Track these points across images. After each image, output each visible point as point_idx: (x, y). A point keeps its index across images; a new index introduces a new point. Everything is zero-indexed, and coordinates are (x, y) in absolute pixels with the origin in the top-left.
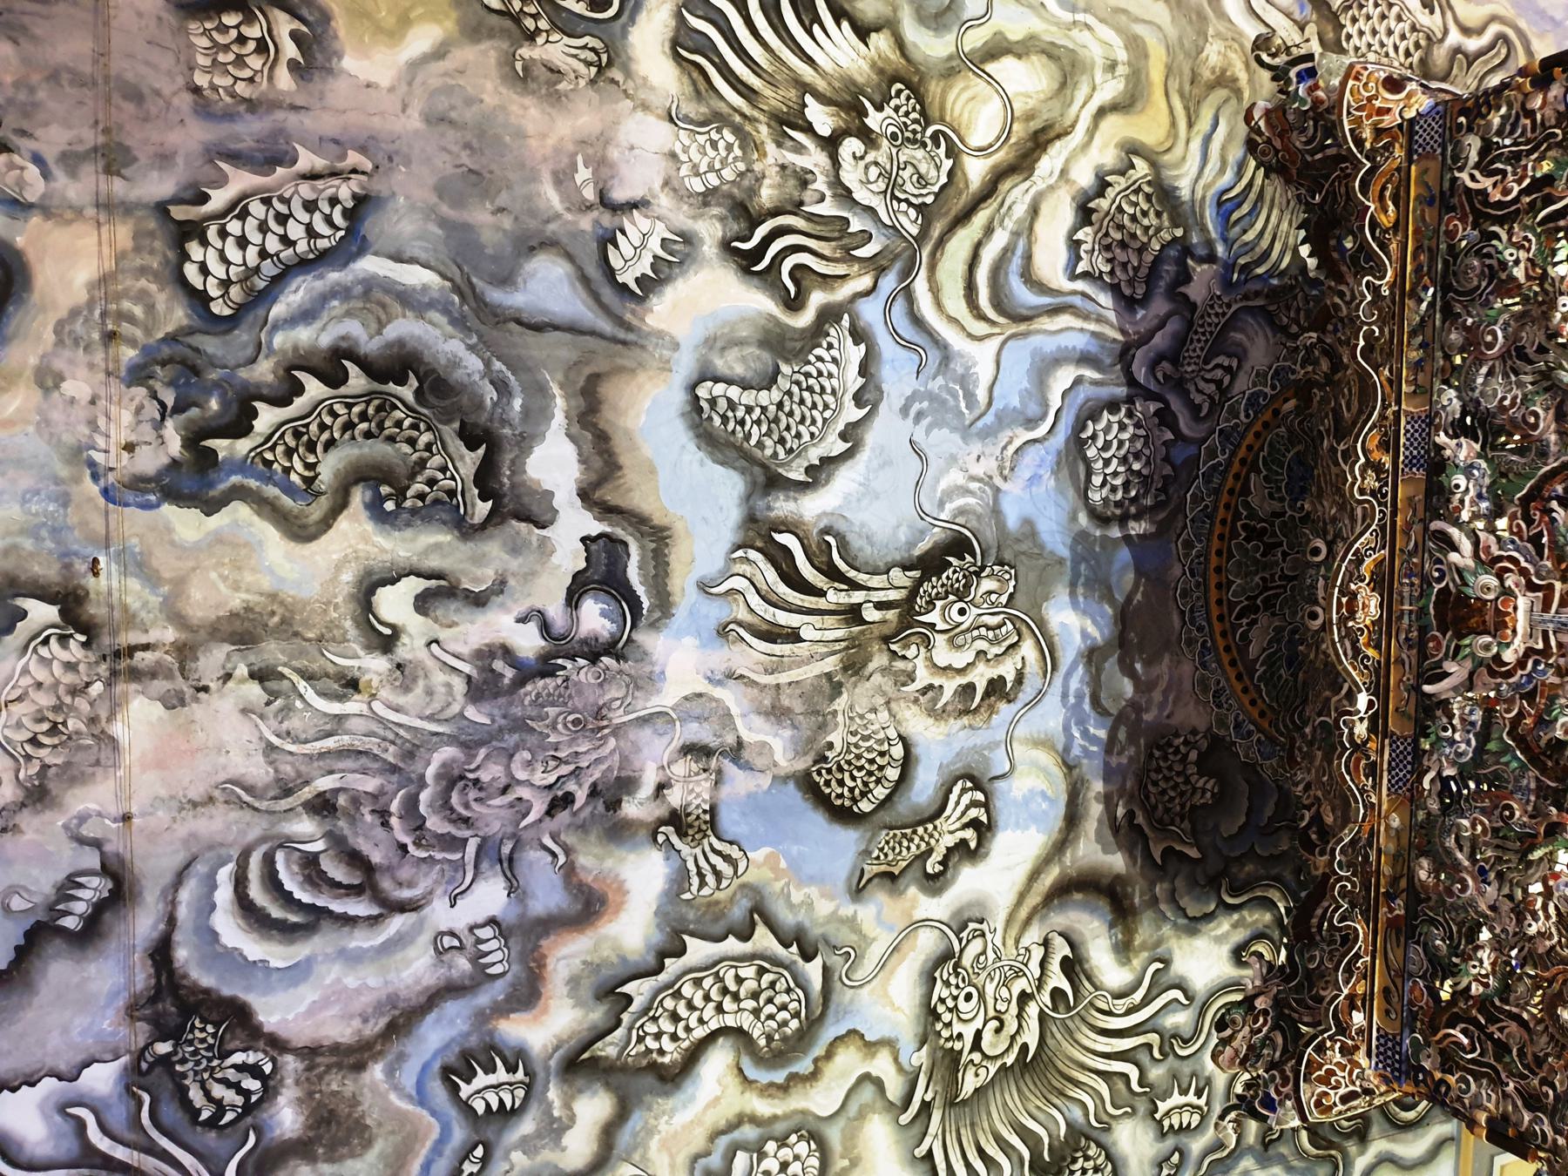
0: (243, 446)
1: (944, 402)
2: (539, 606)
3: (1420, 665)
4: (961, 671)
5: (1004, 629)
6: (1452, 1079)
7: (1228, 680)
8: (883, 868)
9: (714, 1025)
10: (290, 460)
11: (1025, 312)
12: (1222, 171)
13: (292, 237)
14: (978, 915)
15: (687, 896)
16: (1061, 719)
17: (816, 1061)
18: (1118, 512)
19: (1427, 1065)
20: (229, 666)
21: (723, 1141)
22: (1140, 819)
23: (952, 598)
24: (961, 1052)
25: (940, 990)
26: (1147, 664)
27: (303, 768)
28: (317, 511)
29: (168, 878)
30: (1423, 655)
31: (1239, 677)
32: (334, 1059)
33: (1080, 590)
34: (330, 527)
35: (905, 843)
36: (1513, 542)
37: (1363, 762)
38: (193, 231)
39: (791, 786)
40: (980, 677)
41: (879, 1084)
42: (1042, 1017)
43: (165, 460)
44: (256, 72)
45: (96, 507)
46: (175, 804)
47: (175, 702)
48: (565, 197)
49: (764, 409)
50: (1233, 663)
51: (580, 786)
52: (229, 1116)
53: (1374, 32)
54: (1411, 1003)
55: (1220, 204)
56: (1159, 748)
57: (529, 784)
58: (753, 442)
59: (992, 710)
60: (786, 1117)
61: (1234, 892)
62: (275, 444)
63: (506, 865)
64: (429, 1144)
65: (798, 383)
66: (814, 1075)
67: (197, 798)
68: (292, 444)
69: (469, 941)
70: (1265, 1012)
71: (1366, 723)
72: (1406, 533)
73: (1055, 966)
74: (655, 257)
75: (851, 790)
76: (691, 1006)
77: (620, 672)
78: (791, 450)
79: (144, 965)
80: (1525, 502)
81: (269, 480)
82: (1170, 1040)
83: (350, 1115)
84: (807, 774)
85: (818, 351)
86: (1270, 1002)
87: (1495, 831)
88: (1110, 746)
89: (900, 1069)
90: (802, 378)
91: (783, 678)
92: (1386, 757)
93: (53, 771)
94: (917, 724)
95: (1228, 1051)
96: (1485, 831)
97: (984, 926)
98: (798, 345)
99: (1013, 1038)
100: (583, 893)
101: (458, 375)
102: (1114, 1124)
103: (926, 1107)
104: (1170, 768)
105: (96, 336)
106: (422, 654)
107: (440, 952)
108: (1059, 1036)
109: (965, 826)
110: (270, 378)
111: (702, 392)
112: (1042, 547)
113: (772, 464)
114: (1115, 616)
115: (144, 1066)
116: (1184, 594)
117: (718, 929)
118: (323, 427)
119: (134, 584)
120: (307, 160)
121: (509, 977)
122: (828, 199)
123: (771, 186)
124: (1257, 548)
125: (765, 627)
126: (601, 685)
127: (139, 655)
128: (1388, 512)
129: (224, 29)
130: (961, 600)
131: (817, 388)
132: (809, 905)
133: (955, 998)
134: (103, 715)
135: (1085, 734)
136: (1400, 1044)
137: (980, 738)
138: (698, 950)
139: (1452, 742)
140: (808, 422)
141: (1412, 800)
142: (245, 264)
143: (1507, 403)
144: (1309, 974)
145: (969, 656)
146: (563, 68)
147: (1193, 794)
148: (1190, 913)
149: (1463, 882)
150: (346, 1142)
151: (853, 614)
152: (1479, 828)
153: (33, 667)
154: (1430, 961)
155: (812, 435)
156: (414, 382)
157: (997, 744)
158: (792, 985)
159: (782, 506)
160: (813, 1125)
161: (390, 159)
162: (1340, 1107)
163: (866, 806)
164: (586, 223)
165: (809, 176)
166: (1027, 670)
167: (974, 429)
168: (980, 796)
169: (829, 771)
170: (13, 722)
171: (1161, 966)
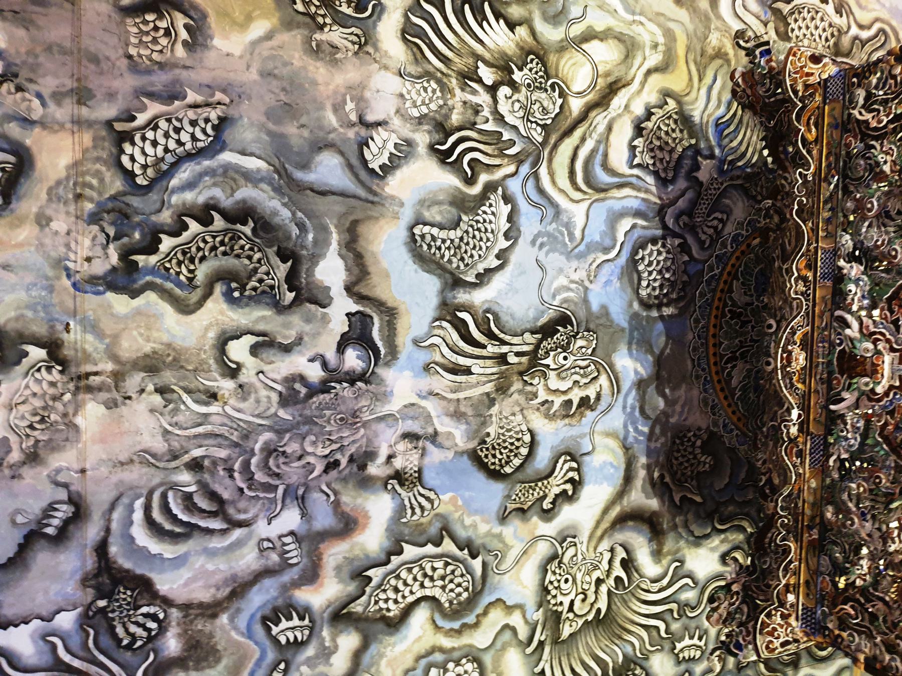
0: (153, 259)
1: (556, 238)
2: (321, 352)
3: (828, 393)
4: (564, 393)
5: (589, 369)
6: (845, 635)
7: (719, 399)
8: (518, 506)
9: (419, 595)
10: (180, 267)
11: (603, 187)
12: (718, 106)
13: (183, 140)
14: (573, 534)
15: (404, 520)
16: (622, 421)
17: (478, 616)
18: (656, 302)
19: (830, 626)
20: (143, 385)
21: (423, 662)
22: (667, 479)
23: (559, 350)
24: (561, 612)
25: (550, 577)
26: (673, 390)
27: (184, 444)
28: (195, 296)
29: (106, 506)
30: (830, 388)
31: (726, 398)
32: (199, 611)
33: (634, 347)
34: (202, 306)
35: (531, 491)
36: (882, 324)
37: (795, 449)
38: (128, 137)
39: (465, 457)
40: (576, 396)
41: (514, 630)
42: (610, 593)
43: (109, 267)
44: (164, 47)
45: (69, 293)
46: (110, 464)
47: (112, 405)
48: (339, 119)
49: (452, 241)
50: (722, 390)
51: (343, 456)
52: (139, 643)
53: (808, 28)
54: (822, 590)
55: (717, 125)
56: (679, 438)
57: (314, 454)
58: (446, 259)
59: (582, 415)
60: (460, 648)
61: (722, 522)
62: (172, 258)
63: (300, 501)
64: (253, 661)
65: (472, 226)
66: (476, 625)
67: (123, 460)
68: (181, 258)
69: (278, 544)
70: (737, 593)
71: (797, 427)
72: (821, 317)
73: (617, 563)
74: (391, 153)
75: (500, 460)
76: (406, 584)
77: (367, 391)
78: (467, 265)
79: (91, 555)
80: (889, 300)
81: (168, 279)
82: (684, 606)
83: (208, 643)
84: (474, 451)
85: (483, 208)
86: (740, 587)
87: (871, 490)
88: (650, 437)
89: (526, 622)
90: (474, 223)
91: (461, 395)
92: (808, 446)
93: (41, 444)
94: (539, 423)
95: (716, 615)
96: (865, 491)
97: (576, 540)
98: (472, 205)
99: (592, 605)
100: (343, 517)
101: (277, 220)
102: (651, 656)
103: (541, 644)
104: (685, 450)
105: (71, 196)
106: (254, 379)
107: (262, 551)
108: (619, 604)
109: (566, 482)
110: (169, 221)
111: (417, 231)
112: (612, 321)
113: (456, 272)
114: (654, 362)
115: (91, 613)
116: (695, 349)
117: (422, 539)
118: (199, 249)
119: (90, 337)
120: (192, 97)
121: (301, 565)
122: (491, 121)
123: (458, 114)
124: (736, 324)
125: (451, 366)
126: (356, 398)
127: (92, 378)
128: (811, 304)
129: (146, 22)
130: (565, 351)
131: (483, 229)
132: (474, 526)
133: (559, 581)
134: (71, 411)
135: (636, 430)
136: (815, 613)
137: (574, 431)
138: (410, 552)
139: (846, 439)
140: (477, 248)
141: (823, 471)
142: (156, 155)
143: (879, 243)
144: (763, 571)
145: (569, 384)
146: (339, 45)
147: (698, 465)
148: (696, 534)
149: (852, 519)
150: (205, 659)
151: (502, 359)
152: (862, 489)
153: (31, 384)
154: (833, 566)
155: (480, 256)
156: (251, 224)
157: (585, 435)
158: (464, 572)
159: (462, 296)
160: (476, 654)
161: (240, 97)
162: (780, 650)
163: (508, 470)
164: (351, 134)
165: (480, 108)
166: (603, 392)
167: (573, 253)
168: (574, 465)
169: (487, 449)
170: (18, 416)
171: (678, 564)
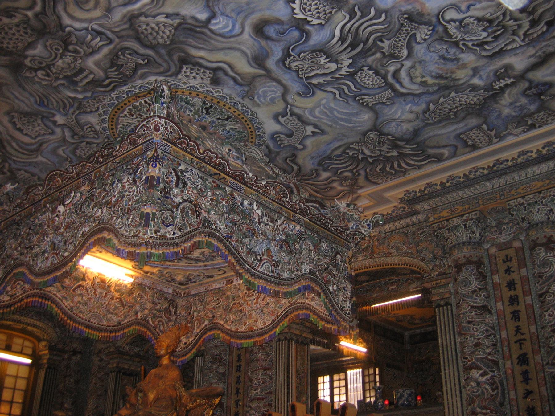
12: (29, 100)
53: (11, 39)
55: (39, 105)
